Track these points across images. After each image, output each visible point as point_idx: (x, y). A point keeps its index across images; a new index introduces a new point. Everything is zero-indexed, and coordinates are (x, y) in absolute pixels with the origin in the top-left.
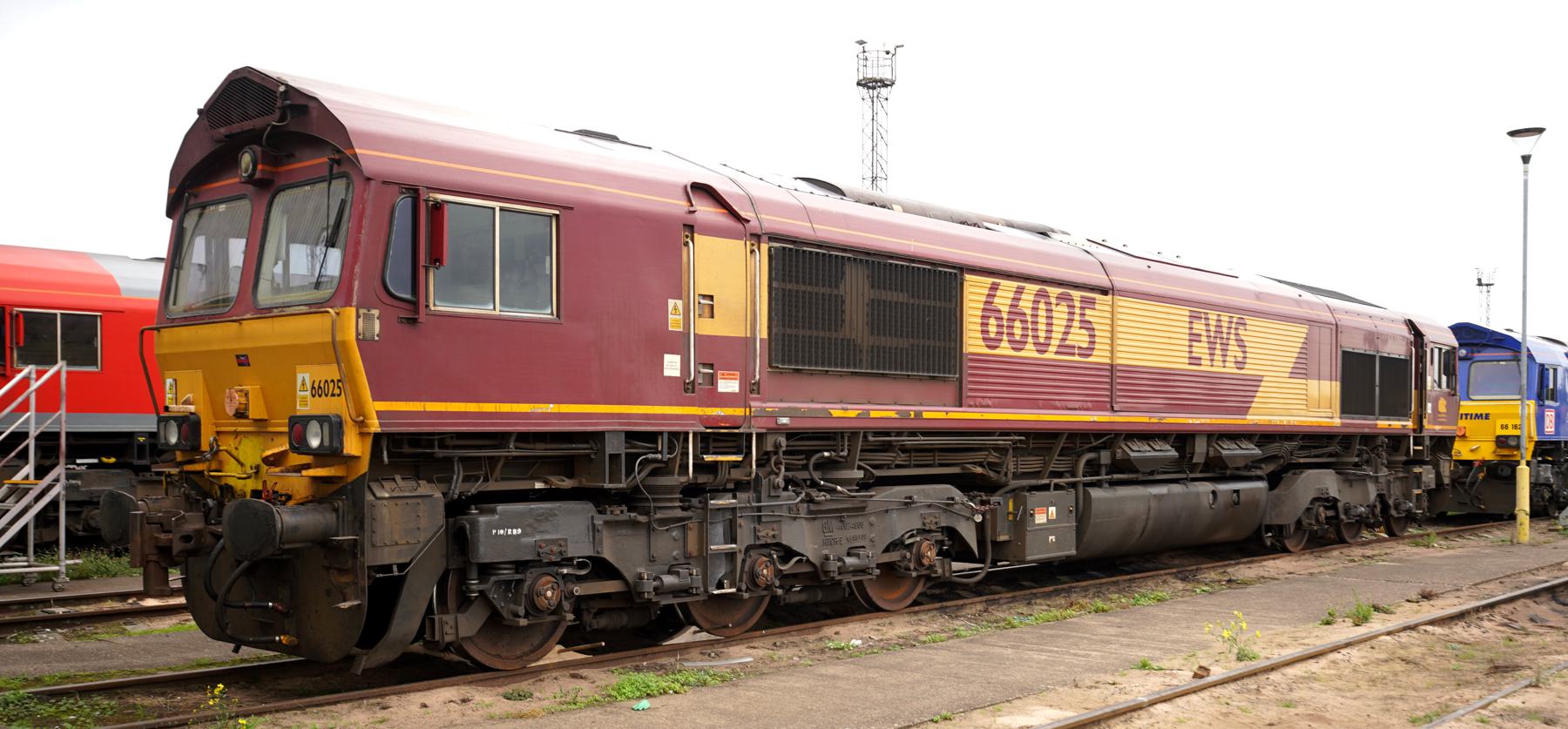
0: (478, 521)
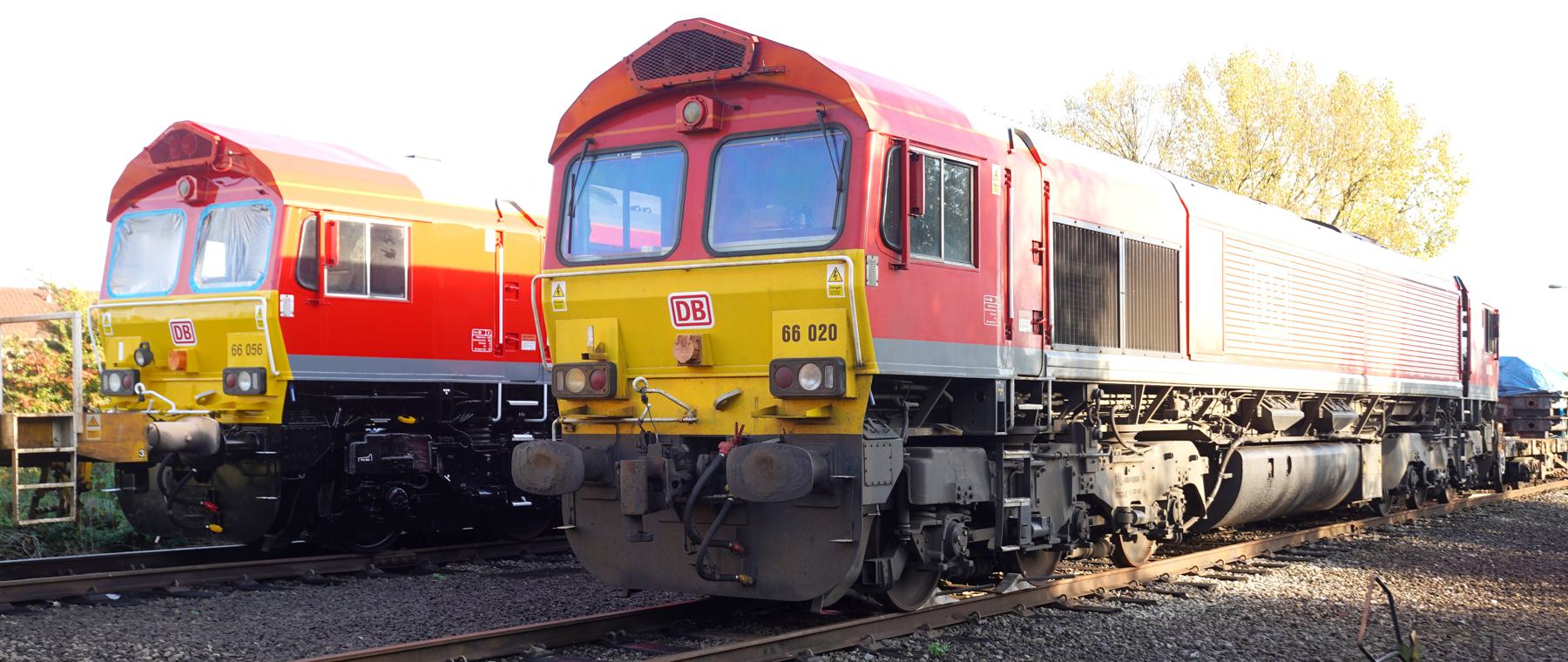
0: (923, 466)
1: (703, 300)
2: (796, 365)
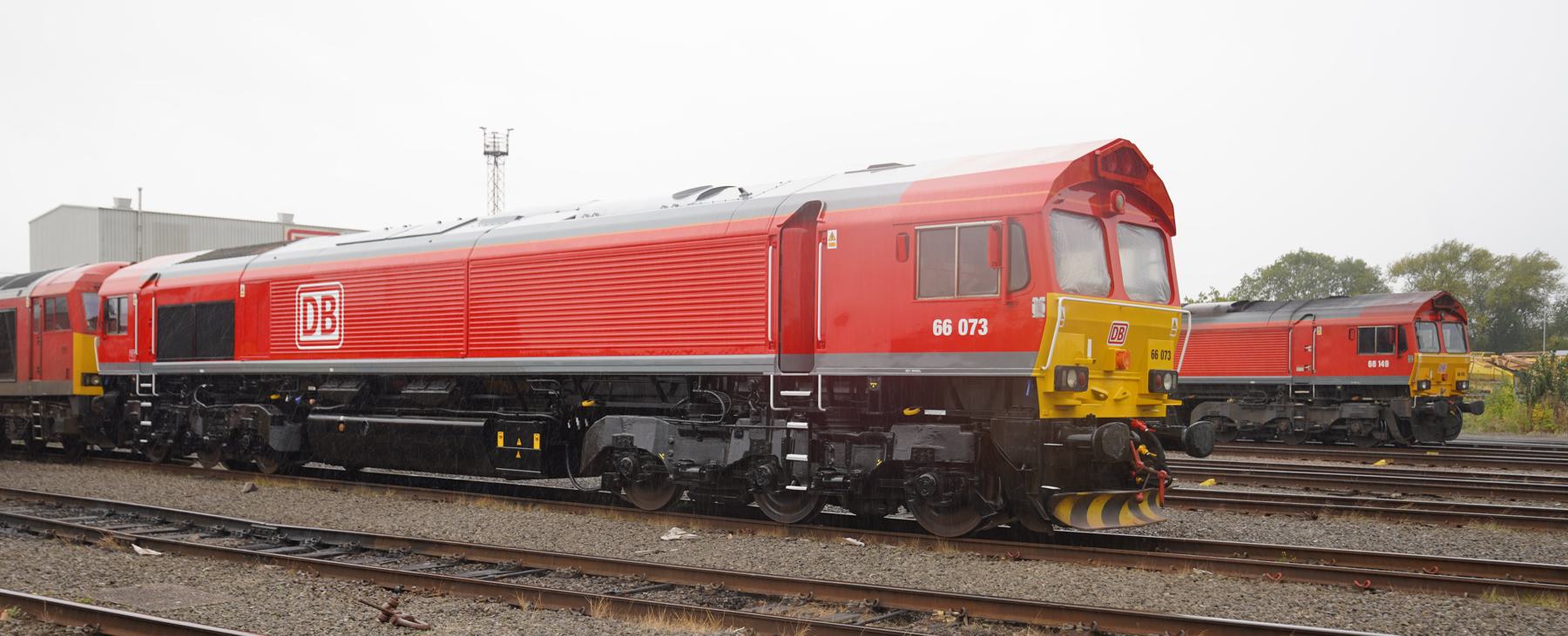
1: (1125, 327)
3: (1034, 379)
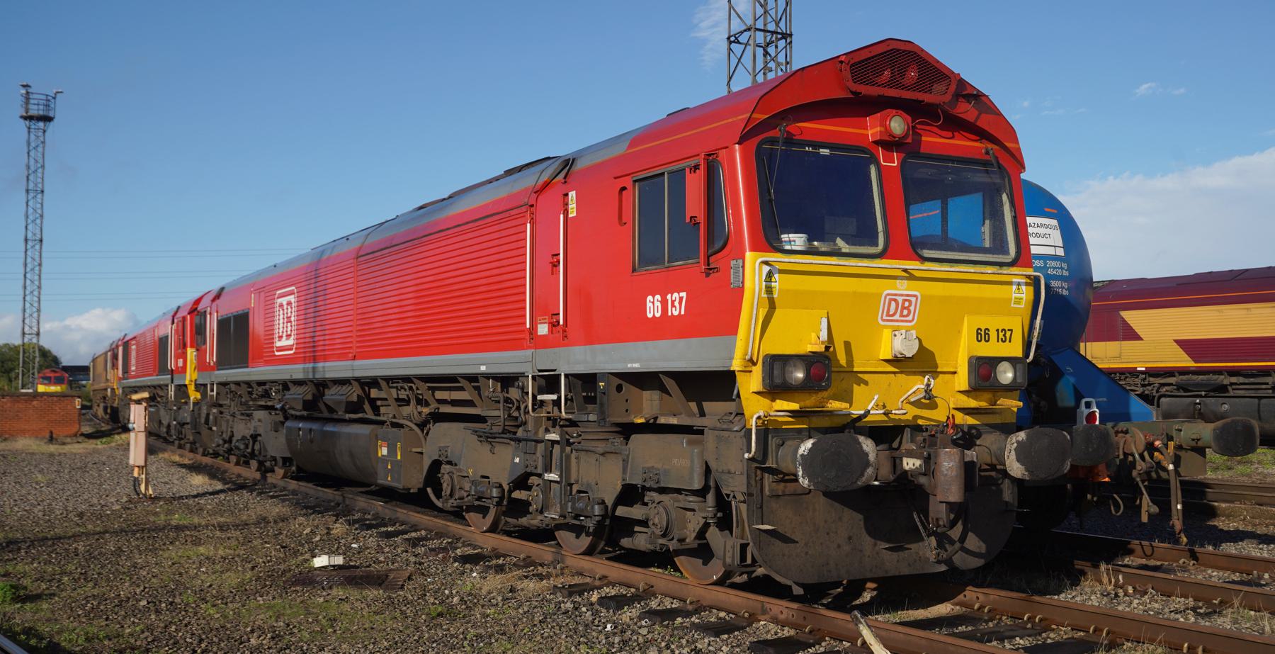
1: (913, 299)
2: (994, 362)
3: (734, 371)
